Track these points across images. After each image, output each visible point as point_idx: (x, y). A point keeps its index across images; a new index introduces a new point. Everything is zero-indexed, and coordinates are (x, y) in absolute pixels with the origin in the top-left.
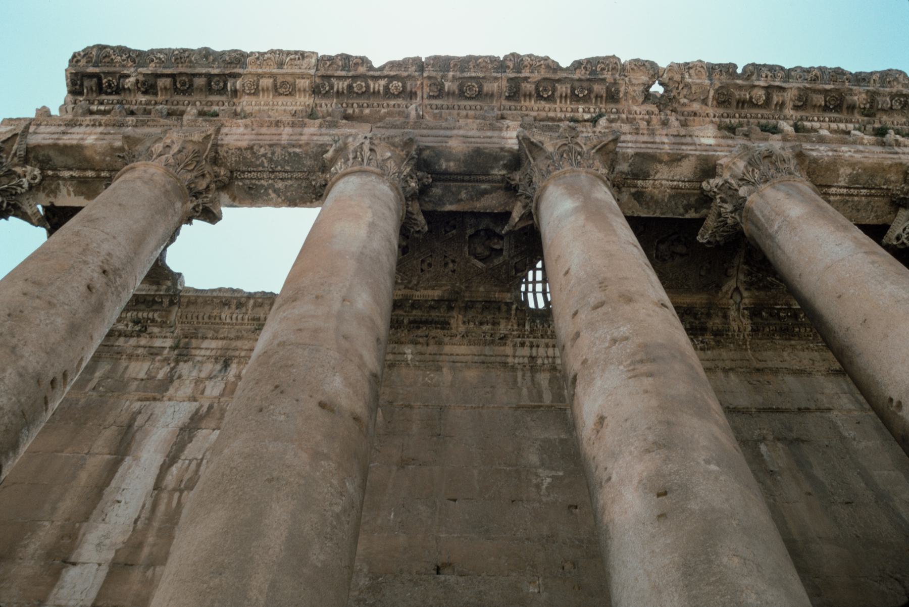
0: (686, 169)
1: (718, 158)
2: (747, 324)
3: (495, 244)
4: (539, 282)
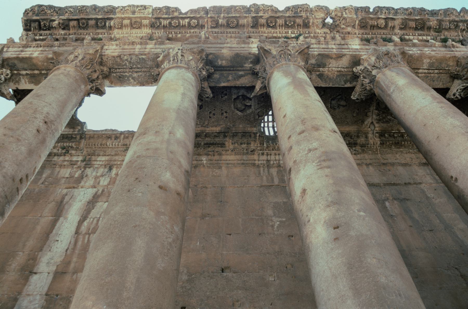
0: (345, 62)
1: (361, 55)
2: (378, 141)
3: (247, 103)
4: (270, 122)
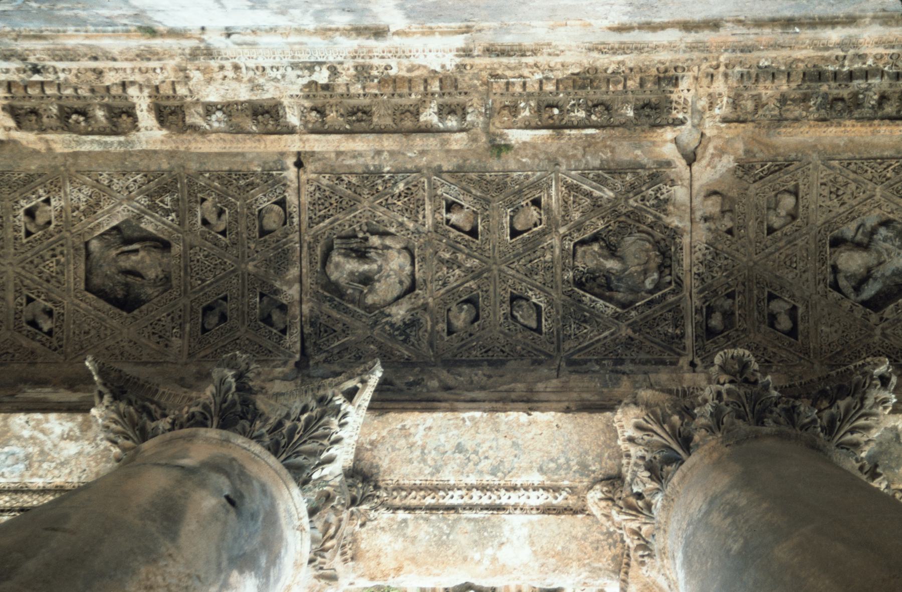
2: (685, 91)
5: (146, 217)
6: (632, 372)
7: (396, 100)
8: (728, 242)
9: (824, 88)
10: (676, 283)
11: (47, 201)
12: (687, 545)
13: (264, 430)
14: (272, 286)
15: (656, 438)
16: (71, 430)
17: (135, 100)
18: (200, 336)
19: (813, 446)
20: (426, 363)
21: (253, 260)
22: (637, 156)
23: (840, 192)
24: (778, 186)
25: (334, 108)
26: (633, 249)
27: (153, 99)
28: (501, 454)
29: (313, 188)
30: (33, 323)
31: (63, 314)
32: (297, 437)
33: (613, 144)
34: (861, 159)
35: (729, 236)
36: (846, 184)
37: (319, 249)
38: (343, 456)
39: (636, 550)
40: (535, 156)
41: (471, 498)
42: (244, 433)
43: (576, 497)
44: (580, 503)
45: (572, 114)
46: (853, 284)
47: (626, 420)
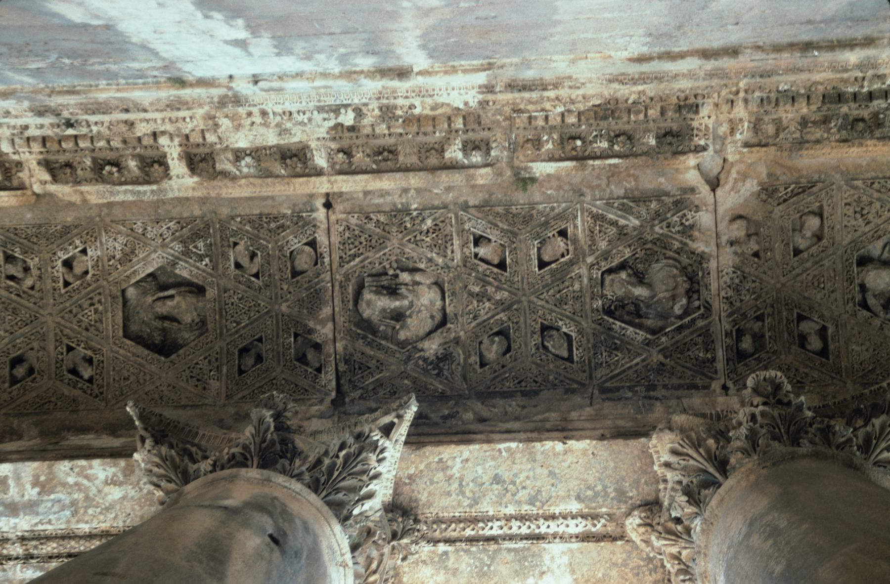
5: (181, 263)
6: (665, 397)
7: (421, 138)
8: (755, 265)
9: (844, 109)
10: (705, 307)
11: (84, 252)
12: (728, 569)
13: (304, 468)
14: (306, 326)
15: (692, 462)
16: (114, 475)
17: (166, 149)
18: (237, 378)
19: (851, 465)
20: (460, 396)
21: (287, 300)
22: (661, 184)
23: (865, 212)
24: (802, 208)
25: (360, 149)
26: (660, 275)
27: (184, 148)
28: (539, 484)
29: (342, 229)
30: (74, 371)
31: (103, 362)
32: (336, 474)
33: (637, 173)
34: (884, 178)
35: (756, 260)
36: (871, 203)
37: (351, 287)
38: (382, 491)
39: (677, 575)
40: (560, 187)
41: (511, 528)
42: (284, 472)
43: (615, 524)
44: (619, 530)
45: (595, 145)
46: (882, 302)
47: (661, 446)
